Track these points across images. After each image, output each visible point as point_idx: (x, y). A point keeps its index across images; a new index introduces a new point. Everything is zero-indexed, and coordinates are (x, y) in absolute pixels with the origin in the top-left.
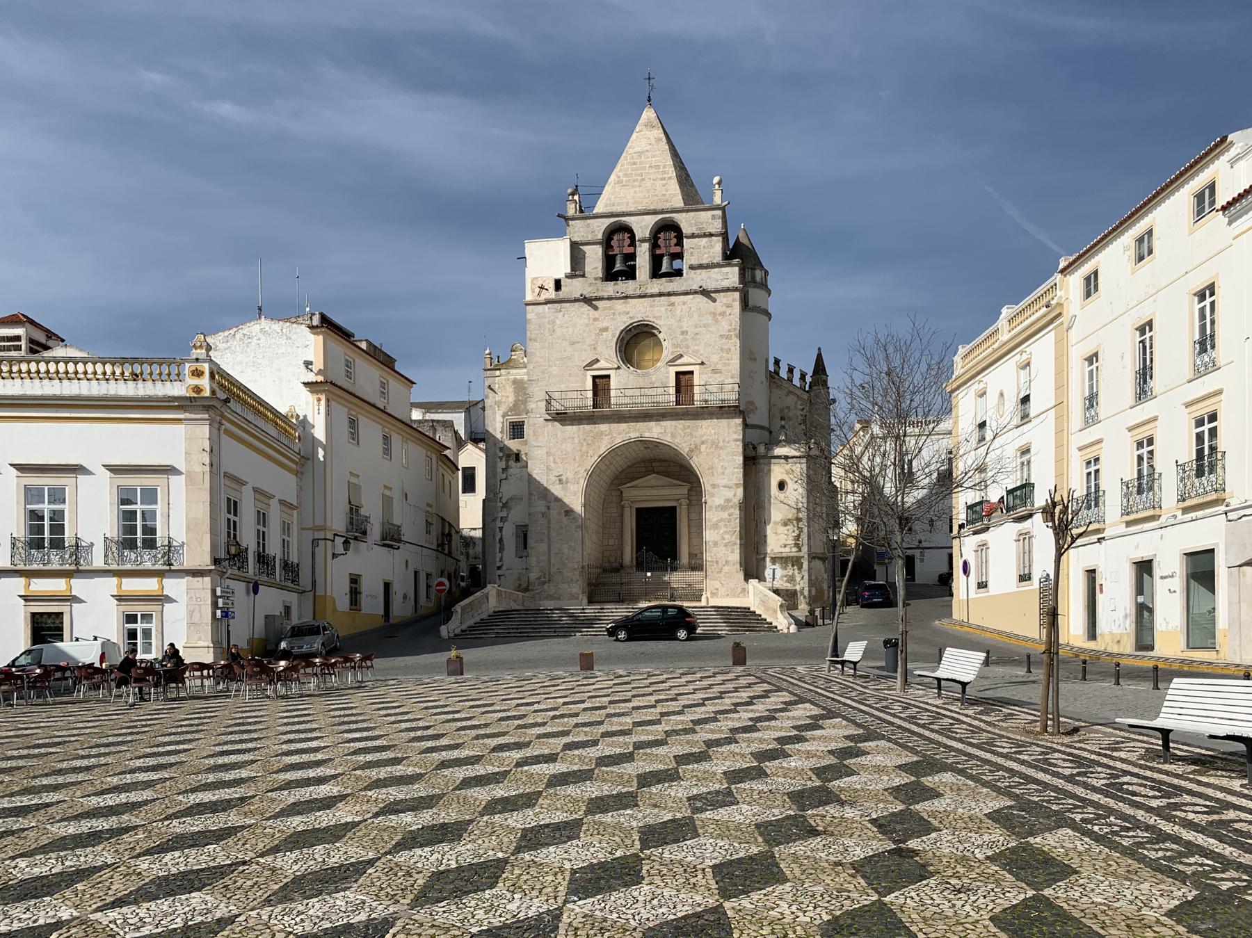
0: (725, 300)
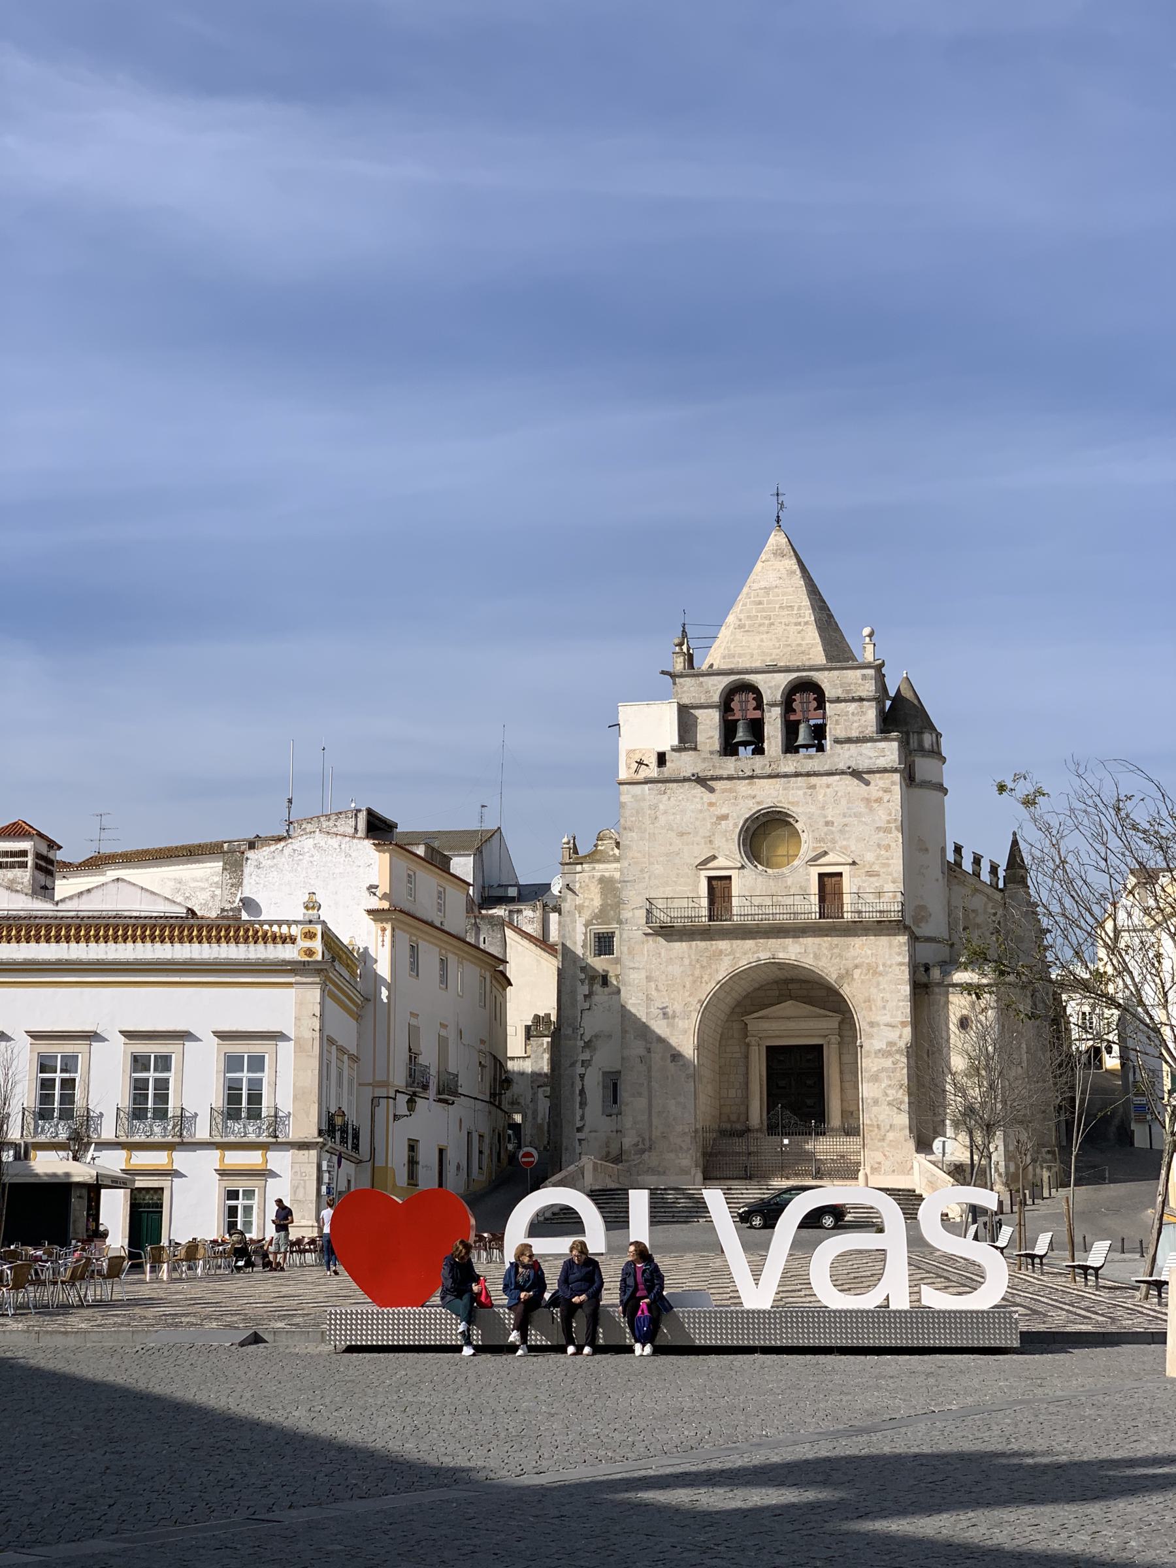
0: (881, 783)
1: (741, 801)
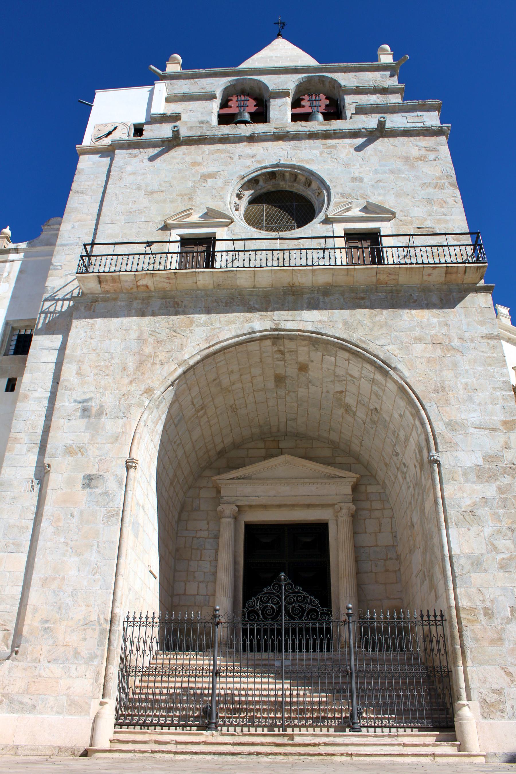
1: (236, 158)
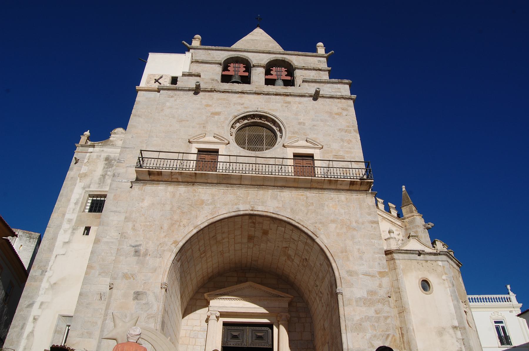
0: (340, 105)
